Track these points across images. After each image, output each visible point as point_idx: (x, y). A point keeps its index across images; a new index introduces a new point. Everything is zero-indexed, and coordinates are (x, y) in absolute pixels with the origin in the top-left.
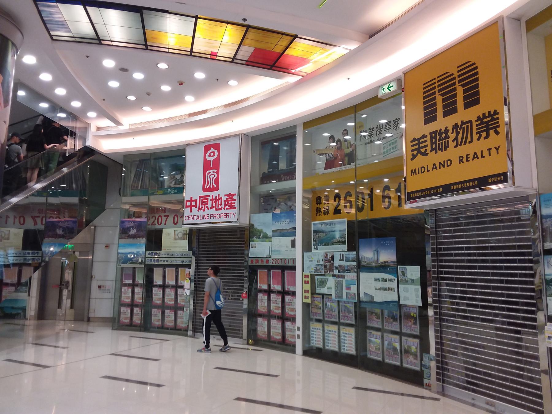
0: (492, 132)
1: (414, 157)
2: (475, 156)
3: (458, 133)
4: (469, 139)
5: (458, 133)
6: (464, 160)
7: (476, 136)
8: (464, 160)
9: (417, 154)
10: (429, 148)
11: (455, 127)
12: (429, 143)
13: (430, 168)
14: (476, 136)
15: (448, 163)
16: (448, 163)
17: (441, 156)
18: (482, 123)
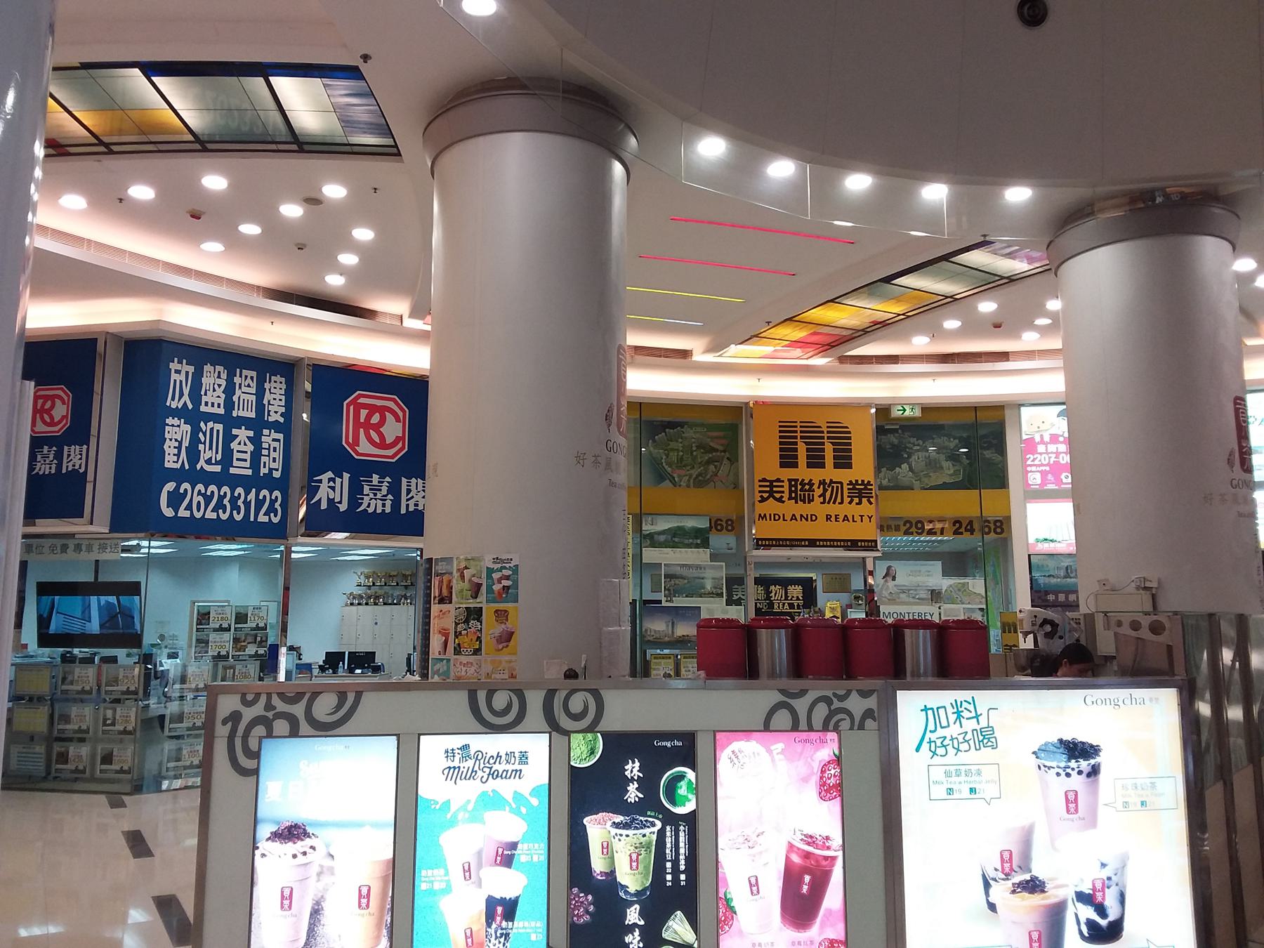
0: (864, 500)
1: (763, 500)
2: (846, 518)
3: (825, 490)
4: (839, 500)
5: (825, 490)
6: (833, 519)
7: (847, 500)
8: (833, 519)
9: (768, 498)
10: (786, 495)
11: (822, 483)
12: (786, 489)
13: (788, 517)
14: (847, 500)
15: (813, 518)
16: (813, 518)
17: (801, 508)
18: (854, 488)
